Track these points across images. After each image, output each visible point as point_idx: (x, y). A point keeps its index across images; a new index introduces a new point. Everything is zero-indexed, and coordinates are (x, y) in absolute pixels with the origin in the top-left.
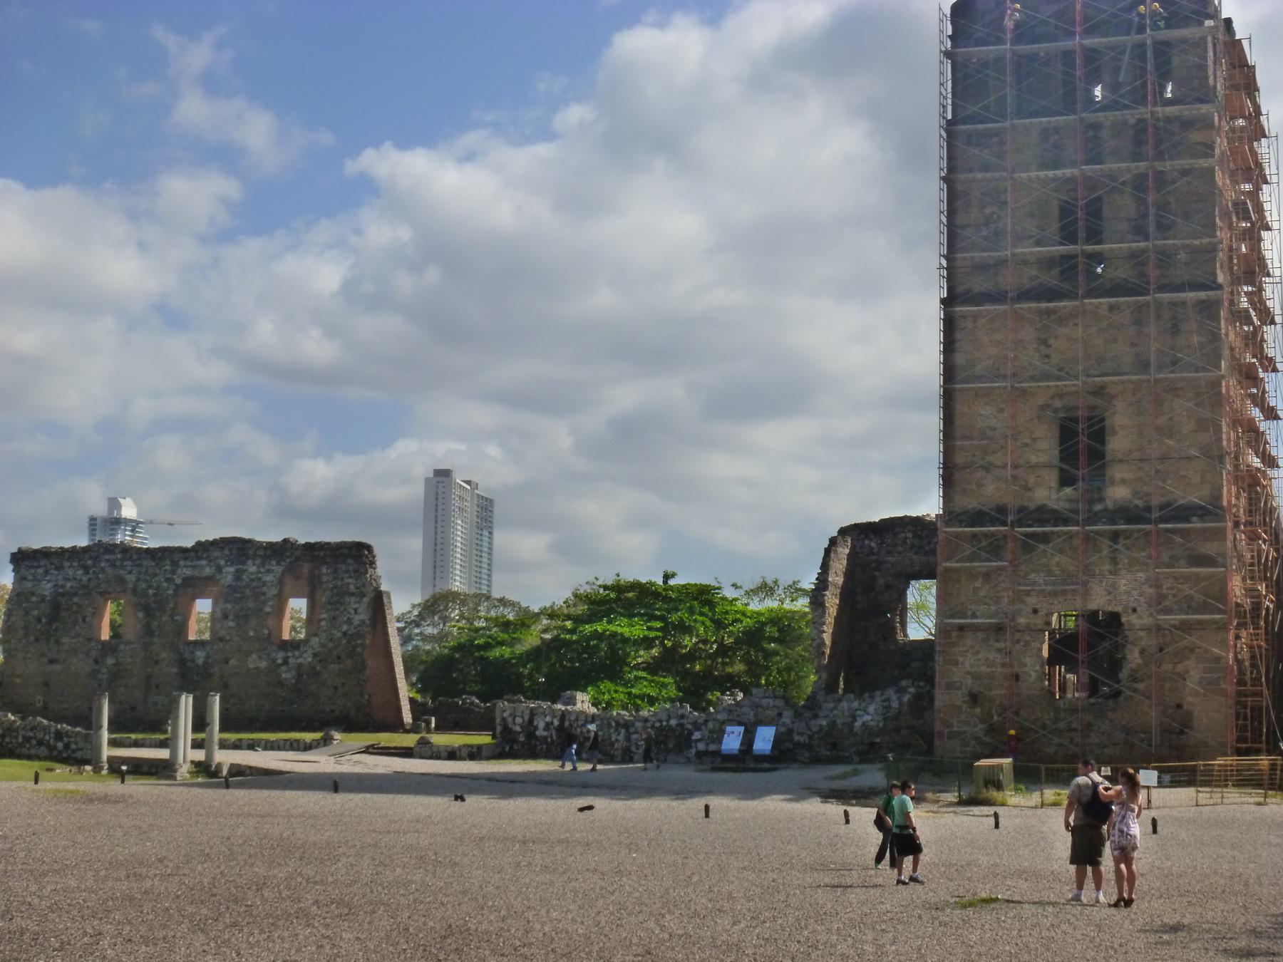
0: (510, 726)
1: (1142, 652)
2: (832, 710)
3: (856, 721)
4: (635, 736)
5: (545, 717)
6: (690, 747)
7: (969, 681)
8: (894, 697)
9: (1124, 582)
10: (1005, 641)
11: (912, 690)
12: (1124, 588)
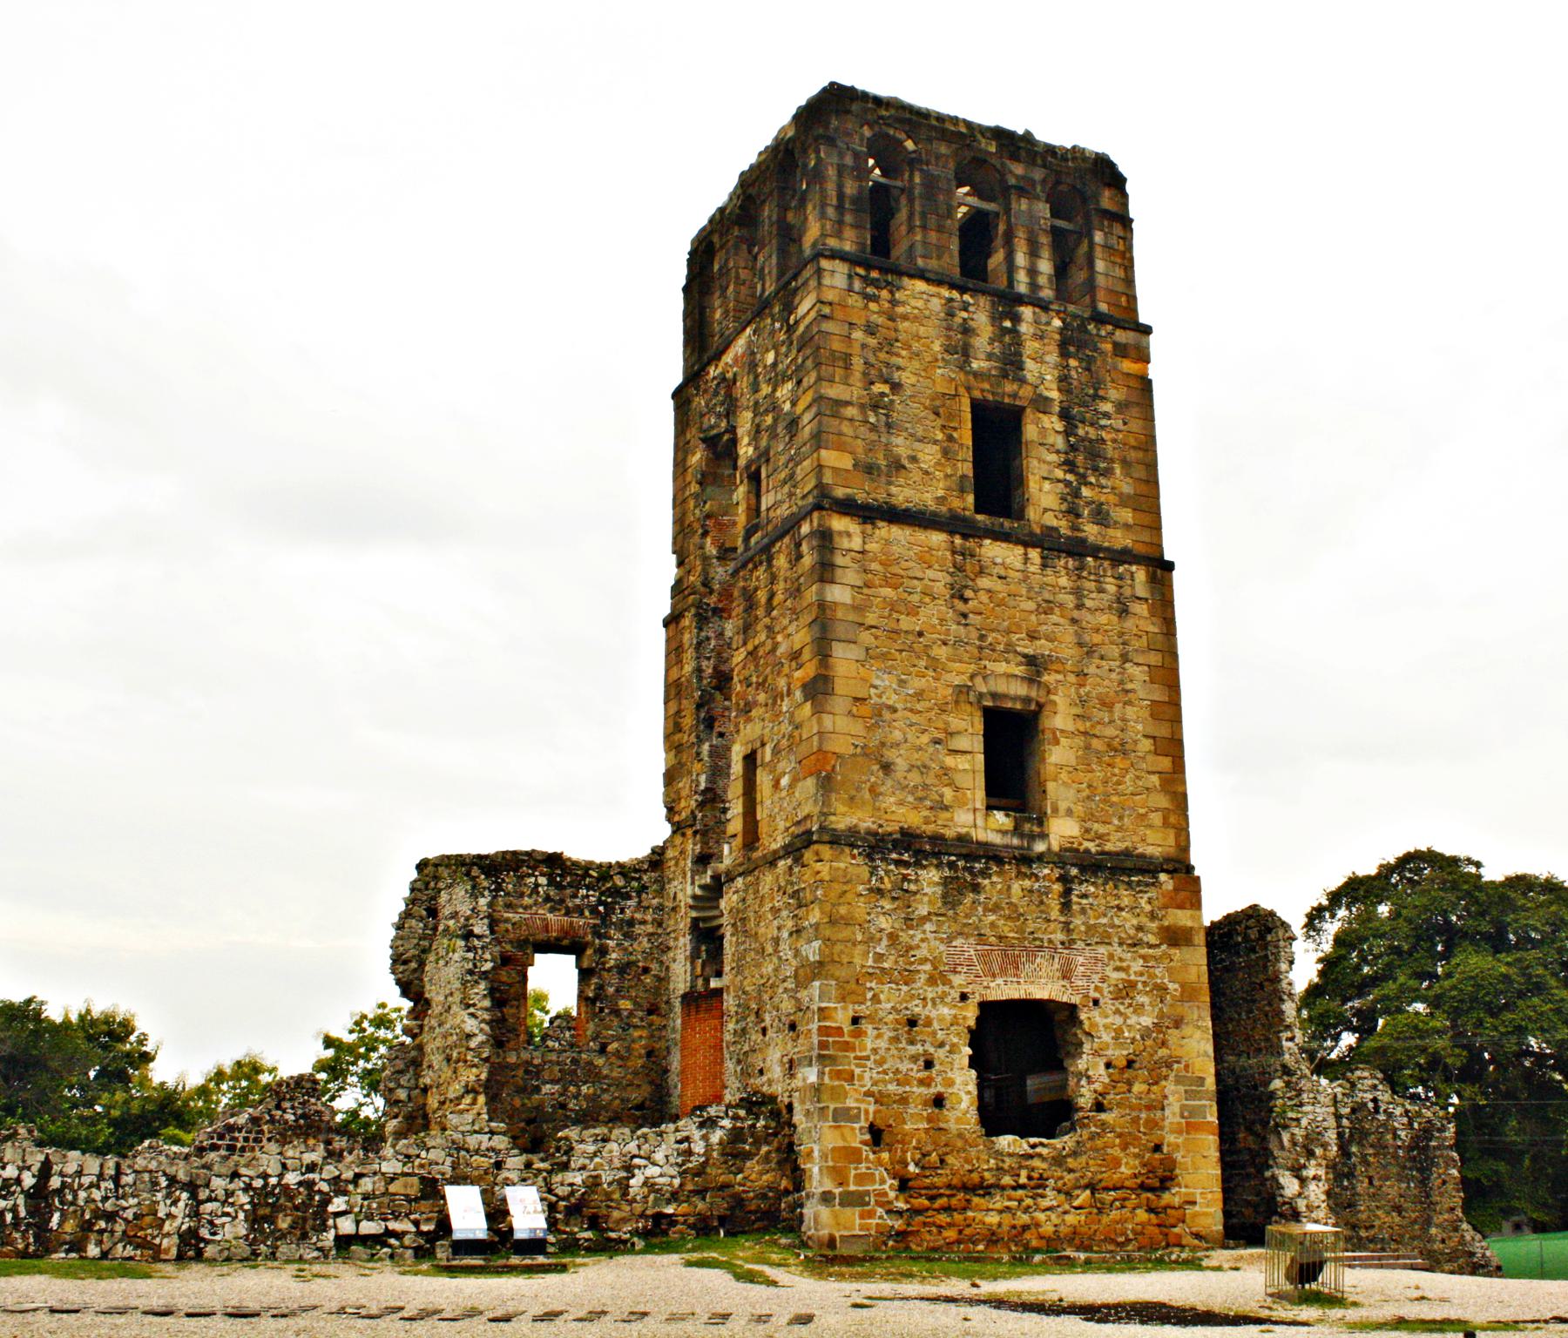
1: (1108, 1065)
2: (595, 1154)
8: (697, 1134)
9: (1081, 959)
11: (726, 1123)
12: (1082, 968)
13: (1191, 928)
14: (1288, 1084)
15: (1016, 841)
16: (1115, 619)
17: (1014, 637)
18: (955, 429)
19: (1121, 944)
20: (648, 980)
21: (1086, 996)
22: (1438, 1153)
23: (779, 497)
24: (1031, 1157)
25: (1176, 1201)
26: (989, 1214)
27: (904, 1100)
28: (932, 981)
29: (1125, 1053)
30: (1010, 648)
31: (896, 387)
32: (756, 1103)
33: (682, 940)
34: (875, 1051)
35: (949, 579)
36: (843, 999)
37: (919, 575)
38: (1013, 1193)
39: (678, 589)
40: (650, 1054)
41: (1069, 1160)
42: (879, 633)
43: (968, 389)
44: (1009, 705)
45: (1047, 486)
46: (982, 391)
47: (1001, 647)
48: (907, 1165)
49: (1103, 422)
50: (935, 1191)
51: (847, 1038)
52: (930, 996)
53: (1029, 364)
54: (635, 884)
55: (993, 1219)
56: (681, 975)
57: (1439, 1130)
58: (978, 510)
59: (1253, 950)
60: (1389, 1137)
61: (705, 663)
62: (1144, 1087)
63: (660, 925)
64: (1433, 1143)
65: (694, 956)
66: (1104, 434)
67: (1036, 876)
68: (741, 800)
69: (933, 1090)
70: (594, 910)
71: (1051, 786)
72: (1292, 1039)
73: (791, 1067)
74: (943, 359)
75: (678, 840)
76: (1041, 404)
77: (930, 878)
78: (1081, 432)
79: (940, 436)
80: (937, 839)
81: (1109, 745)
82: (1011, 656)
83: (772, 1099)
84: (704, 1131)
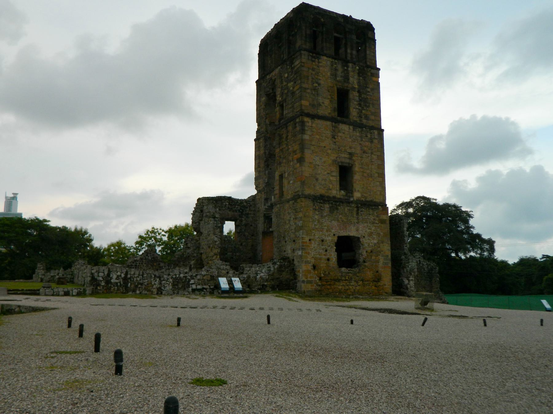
0: (96, 277)
1: (366, 252)
2: (248, 271)
3: (258, 276)
4: (163, 282)
5: (117, 273)
6: (189, 287)
7: (313, 260)
8: (272, 266)
9: (361, 227)
10: (325, 246)
11: (278, 263)
12: (361, 229)
13: (386, 220)
14: (406, 257)
15: (346, 198)
16: (370, 144)
17: (346, 148)
18: (333, 95)
19: (370, 223)
20: (252, 228)
21: (362, 235)
22: (434, 274)
23: (289, 111)
24: (349, 273)
25: (381, 284)
26: (340, 286)
27: (320, 259)
28: (327, 231)
29: (370, 249)
30: (345, 151)
31: (319, 84)
32: (285, 259)
33: (261, 219)
34: (314, 247)
35: (331, 133)
36: (307, 235)
37: (324, 132)
38: (344, 282)
39: (258, 132)
40: (252, 246)
41: (358, 274)
42: (315, 146)
43: (336, 85)
44: (345, 165)
45: (354, 110)
46: (340, 85)
47: (343, 150)
48: (321, 274)
49: (368, 94)
50: (327, 281)
51: (308, 244)
52: (327, 234)
53: (351, 79)
54: (249, 205)
55: (340, 287)
56: (261, 226)
57: (435, 269)
58: (338, 116)
59: (397, 224)
60: (423, 270)
61: (266, 151)
62: (375, 257)
63: (254, 214)
64: (433, 272)
65: (265, 222)
66: (368, 97)
67: (351, 206)
68: (278, 186)
69: (327, 257)
70: (239, 211)
71: (354, 185)
72: (406, 246)
73: (294, 251)
74: (330, 77)
75: (259, 194)
76: (353, 89)
77: (327, 206)
78: (363, 96)
79: (329, 97)
80: (328, 197)
81: (368, 175)
82: (346, 152)
83: (288, 258)
84: (273, 265)
